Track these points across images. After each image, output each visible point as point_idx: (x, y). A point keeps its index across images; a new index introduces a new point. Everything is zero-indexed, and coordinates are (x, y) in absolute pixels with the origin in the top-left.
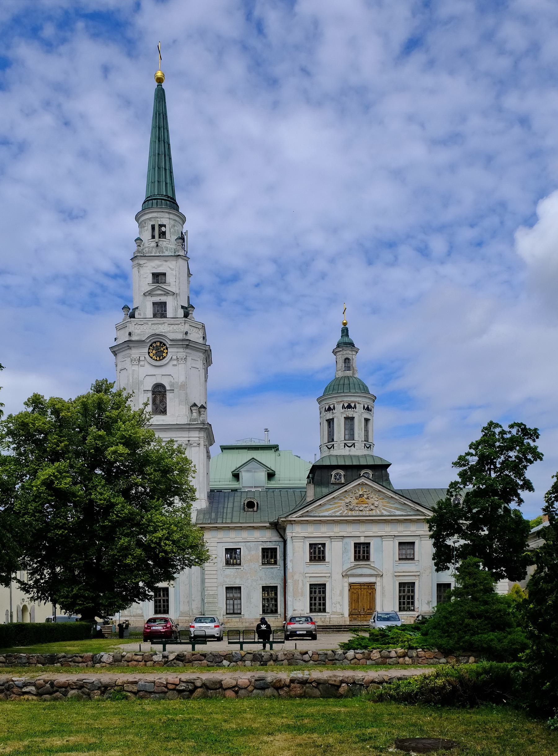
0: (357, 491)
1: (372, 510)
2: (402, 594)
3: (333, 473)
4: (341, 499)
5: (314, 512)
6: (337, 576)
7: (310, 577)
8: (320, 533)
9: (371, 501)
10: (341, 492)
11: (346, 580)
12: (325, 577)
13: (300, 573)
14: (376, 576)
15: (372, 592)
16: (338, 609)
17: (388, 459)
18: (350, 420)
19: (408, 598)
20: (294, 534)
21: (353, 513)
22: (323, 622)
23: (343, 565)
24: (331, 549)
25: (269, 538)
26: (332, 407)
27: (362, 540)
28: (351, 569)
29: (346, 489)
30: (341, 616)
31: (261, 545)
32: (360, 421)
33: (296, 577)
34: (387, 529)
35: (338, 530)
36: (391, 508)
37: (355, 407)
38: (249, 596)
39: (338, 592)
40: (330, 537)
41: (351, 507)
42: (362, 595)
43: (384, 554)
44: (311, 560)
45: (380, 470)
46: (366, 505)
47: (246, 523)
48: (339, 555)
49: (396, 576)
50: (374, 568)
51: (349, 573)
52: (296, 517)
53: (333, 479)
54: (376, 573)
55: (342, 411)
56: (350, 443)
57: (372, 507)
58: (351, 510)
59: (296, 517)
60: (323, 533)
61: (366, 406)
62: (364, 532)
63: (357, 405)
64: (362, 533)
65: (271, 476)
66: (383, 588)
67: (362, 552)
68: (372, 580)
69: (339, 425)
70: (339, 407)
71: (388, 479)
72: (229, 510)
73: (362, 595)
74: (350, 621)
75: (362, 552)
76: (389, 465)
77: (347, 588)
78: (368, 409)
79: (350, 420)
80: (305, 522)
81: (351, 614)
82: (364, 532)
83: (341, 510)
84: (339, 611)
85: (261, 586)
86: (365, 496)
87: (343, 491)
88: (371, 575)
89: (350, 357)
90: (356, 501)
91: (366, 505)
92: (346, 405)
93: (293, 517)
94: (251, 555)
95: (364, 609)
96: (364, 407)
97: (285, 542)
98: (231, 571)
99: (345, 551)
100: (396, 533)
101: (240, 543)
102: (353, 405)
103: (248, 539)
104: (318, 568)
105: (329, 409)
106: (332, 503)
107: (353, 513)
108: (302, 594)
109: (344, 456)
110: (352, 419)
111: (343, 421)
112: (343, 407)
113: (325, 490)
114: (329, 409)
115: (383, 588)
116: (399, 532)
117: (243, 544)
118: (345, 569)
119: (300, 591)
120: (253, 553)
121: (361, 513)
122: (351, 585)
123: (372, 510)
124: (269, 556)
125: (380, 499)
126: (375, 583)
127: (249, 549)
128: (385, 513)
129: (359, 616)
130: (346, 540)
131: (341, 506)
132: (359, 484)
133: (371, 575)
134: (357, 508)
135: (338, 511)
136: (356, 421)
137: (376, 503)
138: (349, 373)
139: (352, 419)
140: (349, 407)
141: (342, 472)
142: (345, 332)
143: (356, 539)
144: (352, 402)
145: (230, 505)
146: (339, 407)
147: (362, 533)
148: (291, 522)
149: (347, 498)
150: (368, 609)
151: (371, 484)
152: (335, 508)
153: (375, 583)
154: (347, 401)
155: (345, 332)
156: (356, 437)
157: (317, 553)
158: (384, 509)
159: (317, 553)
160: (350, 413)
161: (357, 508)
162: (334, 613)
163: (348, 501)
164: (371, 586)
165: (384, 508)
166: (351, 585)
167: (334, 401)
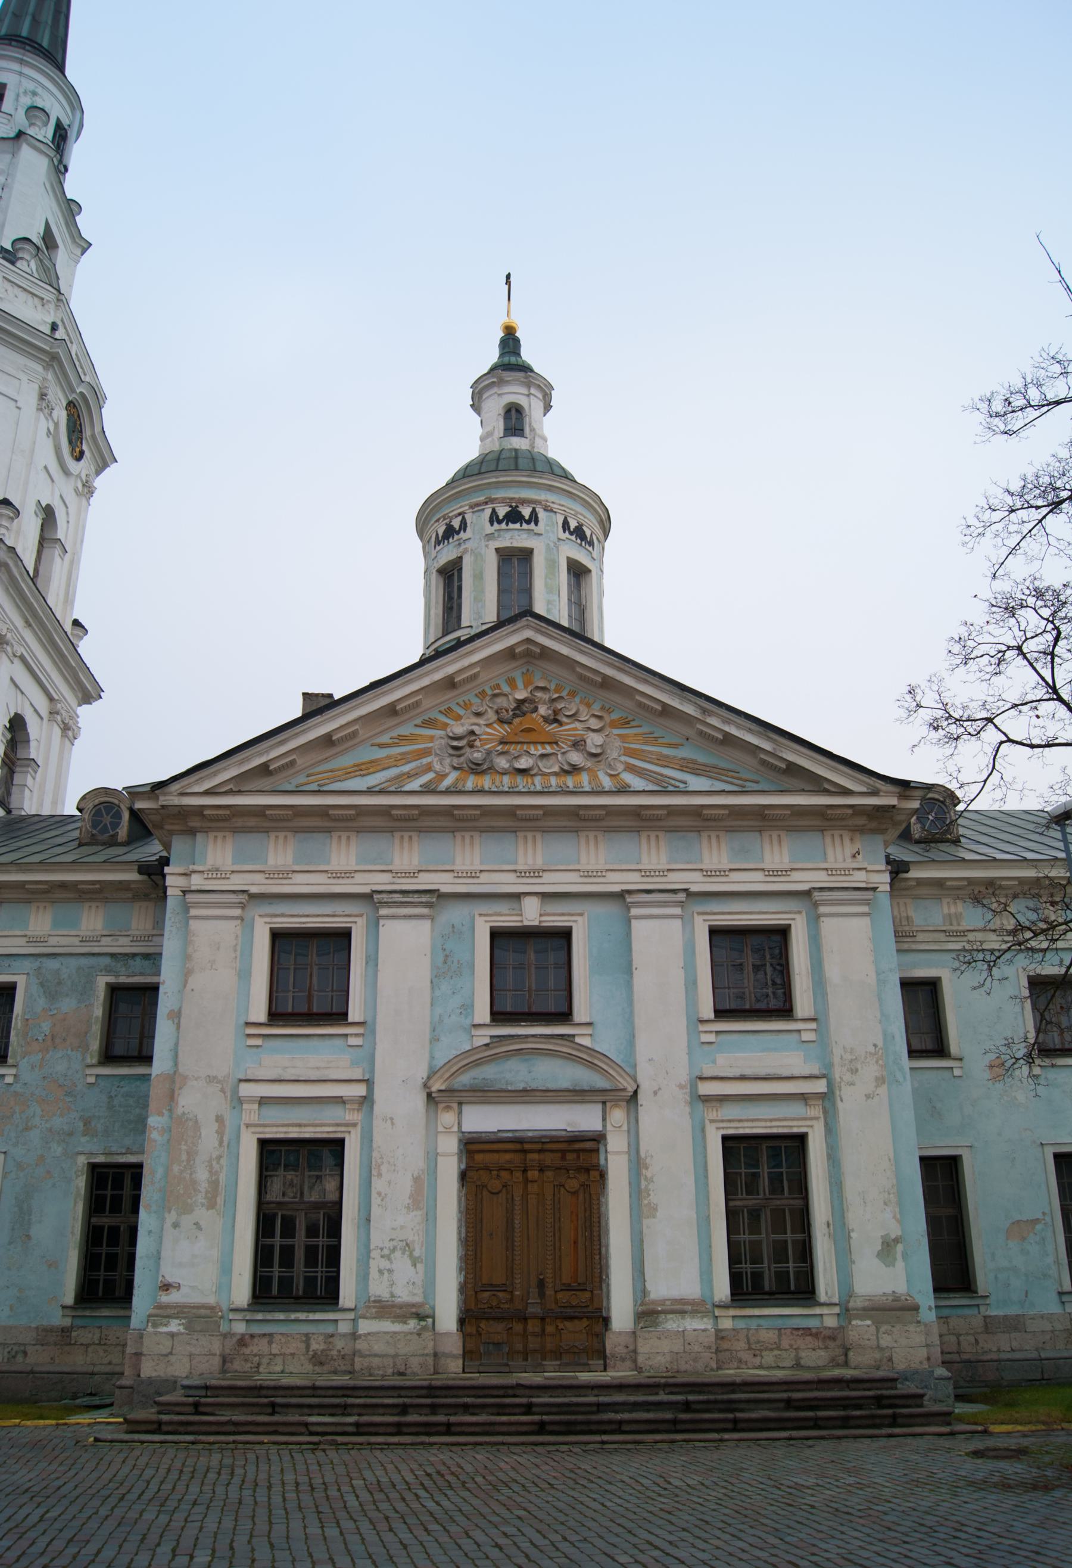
0: (506, 689)
1: (574, 770)
2: (744, 1201)
4: (430, 723)
5: (302, 779)
6: (399, 1101)
7: (263, 1101)
8: (321, 878)
9: (571, 729)
10: (426, 682)
11: (448, 1118)
12: (340, 1100)
13: (211, 1079)
15: (585, 1186)
16: (400, 1282)
19: (779, 1226)
20: (197, 882)
22: (318, 1360)
23: (434, 1040)
24: (372, 960)
26: (456, 523)
27: (531, 914)
28: (474, 1059)
29: (450, 670)
30: (412, 1324)
31: (108, 971)
32: (552, 564)
33: (188, 1101)
34: (652, 860)
35: (409, 860)
36: (664, 761)
37: (534, 518)
39: (405, 1186)
40: (368, 897)
41: (477, 756)
42: (534, 1202)
43: (648, 989)
44: (275, 1016)
46: (548, 749)
47: (44, 865)
48: (414, 986)
49: (706, 1099)
50: (590, 1059)
51: (465, 1079)
52: (208, 793)
54: (601, 1083)
55: (489, 529)
57: (575, 758)
58: (476, 769)
59: (208, 793)
60: (337, 875)
61: (573, 524)
62: (536, 873)
63: (542, 514)
64: (533, 876)
66: (637, 1164)
67: (532, 975)
68: (583, 1119)
69: (479, 577)
73: (534, 1202)
74: (467, 1354)
75: (532, 975)
77: (449, 1169)
80: (252, 822)
82: (536, 873)
83: (429, 768)
84: (404, 1295)
85: (82, 1160)
86: (543, 710)
87: (438, 676)
88: (577, 1095)
89: (523, 401)
90: (501, 730)
91: (548, 749)
92: (502, 511)
95: (541, 1284)
96: (566, 525)
99: (446, 967)
100: (697, 883)
101: (17, 964)
102: (526, 512)
103: (53, 941)
104: (311, 1059)
105: (450, 532)
106: (385, 739)
107: (486, 782)
108: (217, 1196)
110: (525, 555)
112: (494, 518)
114: (450, 532)
115: (637, 1164)
116: (707, 873)
117: (28, 965)
118: (440, 1062)
119: (202, 1175)
120: (67, 1005)
122: (473, 1146)
123: (574, 770)
125: (613, 724)
126: (598, 1139)
127: (51, 990)
129: (518, 1327)
130: (455, 913)
131: (426, 753)
132: (510, 654)
134: (502, 763)
135: (410, 776)
137: (594, 741)
138: (516, 442)
139: (525, 555)
140: (513, 516)
142: (510, 341)
143: (503, 907)
144: (524, 502)
147: (533, 876)
149: (458, 718)
150: (568, 1288)
151: (565, 650)
152: (404, 758)
153: (598, 1139)
154: (503, 501)
155: (510, 341)
157: (310, 976)
158: (630, 769)
159: (310, 976)
160: (516, 537)
161: (502, 763)
162: (384, 1309)
163: (459, 729)
166: (473, 1146)
167: (463, 505)
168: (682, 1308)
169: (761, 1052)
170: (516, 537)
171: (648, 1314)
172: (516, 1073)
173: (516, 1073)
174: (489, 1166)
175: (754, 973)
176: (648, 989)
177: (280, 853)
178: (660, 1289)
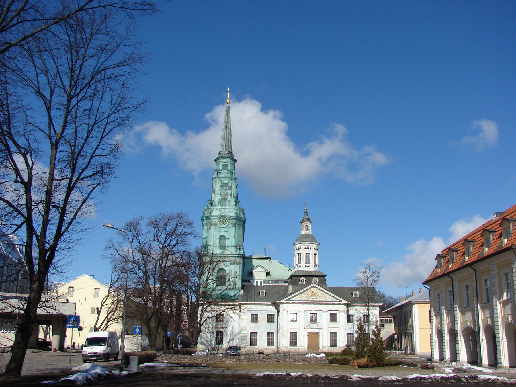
3: (300, 279)
9: (318, 294)
14: (319, 329)
17: (325, 273)
18: (308, 254)
21: (310, 300)
25: (271, 309)
27: (313, 312)
28: (308, 325)
38: (261, 337)
43: (324, 319)
45: (322, 278)
48: (303, 319)
53: (300, 282)
56: (308, 265)
65: (268, 274)
70: (303, 248)
71: (325, 283)
72: (253, 295)
76: (325, 276)
77: (306, 334)
78: (316, 249)
79: (308, 254)
81: (309, 347)
88: (318, 329)
93: (282, 301)
94: (263, 318)
97: (278, 312)
98: (253, 324)
99: (306, 317)
108: (287, 337)
109: (305, 271)
111: (305, 254)
112: (305, 248)
113: (297, 287)
114: (299, 249)
120: (263, 316)
121: (313, 300)
124: (271, 318)
126: (319, 333)
127: (262, 314)
128: (324, 300)
133: (318, 329)
136: (311, 255)
139: (309, 254)
140: (308, 248)
141: (304, 279)
145: (253, 293)
146: (303, 248)
148: (282, 303)
153: (319, 333)
156: (311, 262)
160: (308, 251)
162: (301, 346)
164: (317, 334)
165: (323, 295)
168: (325, 347)
169: (333, 324)
170: (308, 251)
171: (323, 347)
172: (312, 326)
173: (312, 326)
174: (310, 335)
175: (333, 318)
176: (324, 319)
177: (290, 306)
178: (324, 345)
